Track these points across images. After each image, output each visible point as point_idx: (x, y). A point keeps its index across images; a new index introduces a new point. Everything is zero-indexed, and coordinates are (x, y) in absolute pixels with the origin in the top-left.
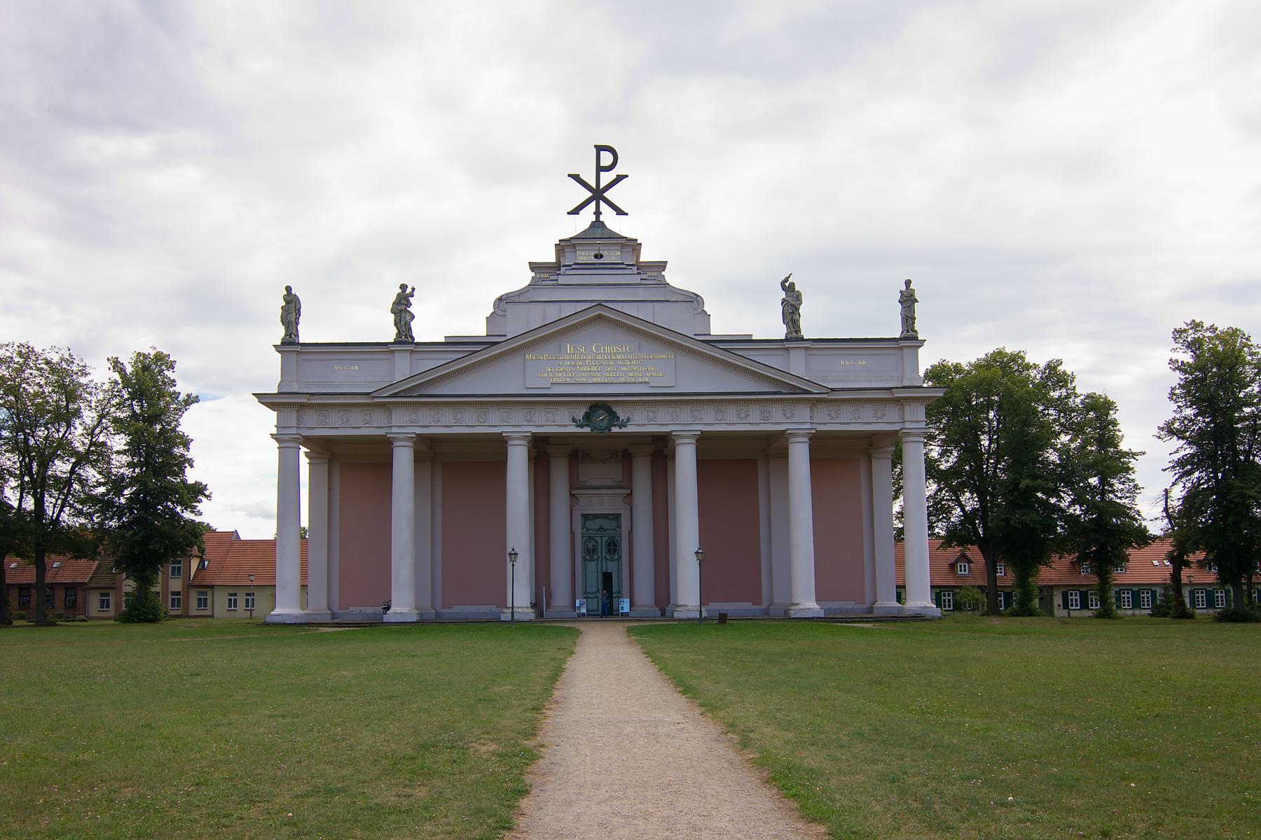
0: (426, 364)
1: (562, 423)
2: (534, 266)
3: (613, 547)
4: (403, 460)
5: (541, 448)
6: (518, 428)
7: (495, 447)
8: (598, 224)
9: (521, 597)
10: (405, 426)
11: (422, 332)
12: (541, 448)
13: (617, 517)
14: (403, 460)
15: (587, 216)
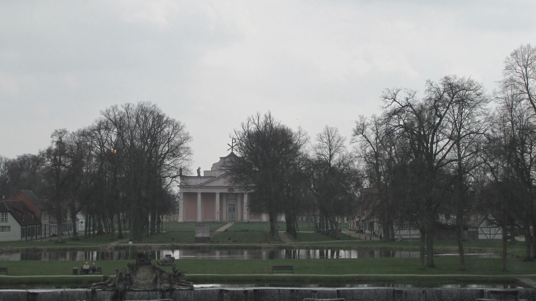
0: (203, 181)
1: (225, 191)
2: (221, 158)
3: (234, 209)
4: (199, 196)
5: (221, 194)
6: (218, 191)
7: (214, 194)
8: (232, 153)
9: (217, 218)
10: (199, 191)
11: (202, 174)
12: (221, 194)
13: (234, 205)
14: (199, 196)
15: (230, 151)
